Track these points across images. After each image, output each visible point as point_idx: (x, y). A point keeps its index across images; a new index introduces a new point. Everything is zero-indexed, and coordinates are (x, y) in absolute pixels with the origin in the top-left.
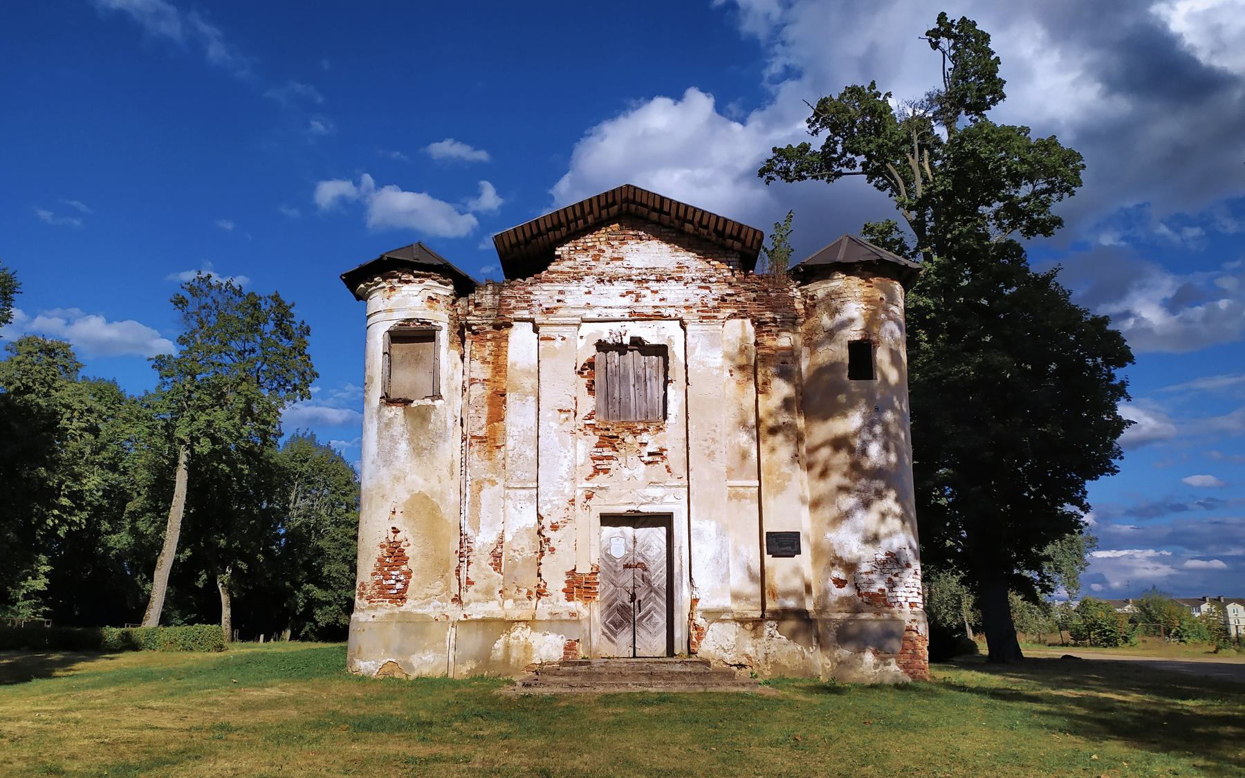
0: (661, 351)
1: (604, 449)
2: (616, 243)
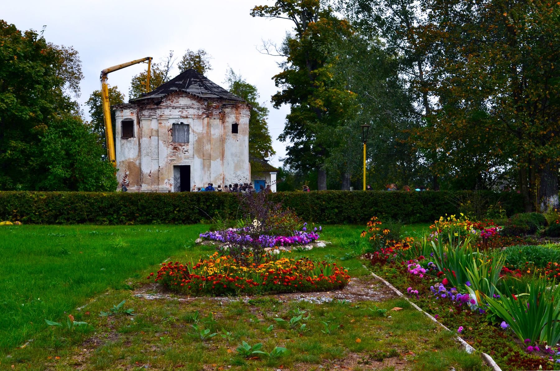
0: (188, 125)
2: (177, 98)
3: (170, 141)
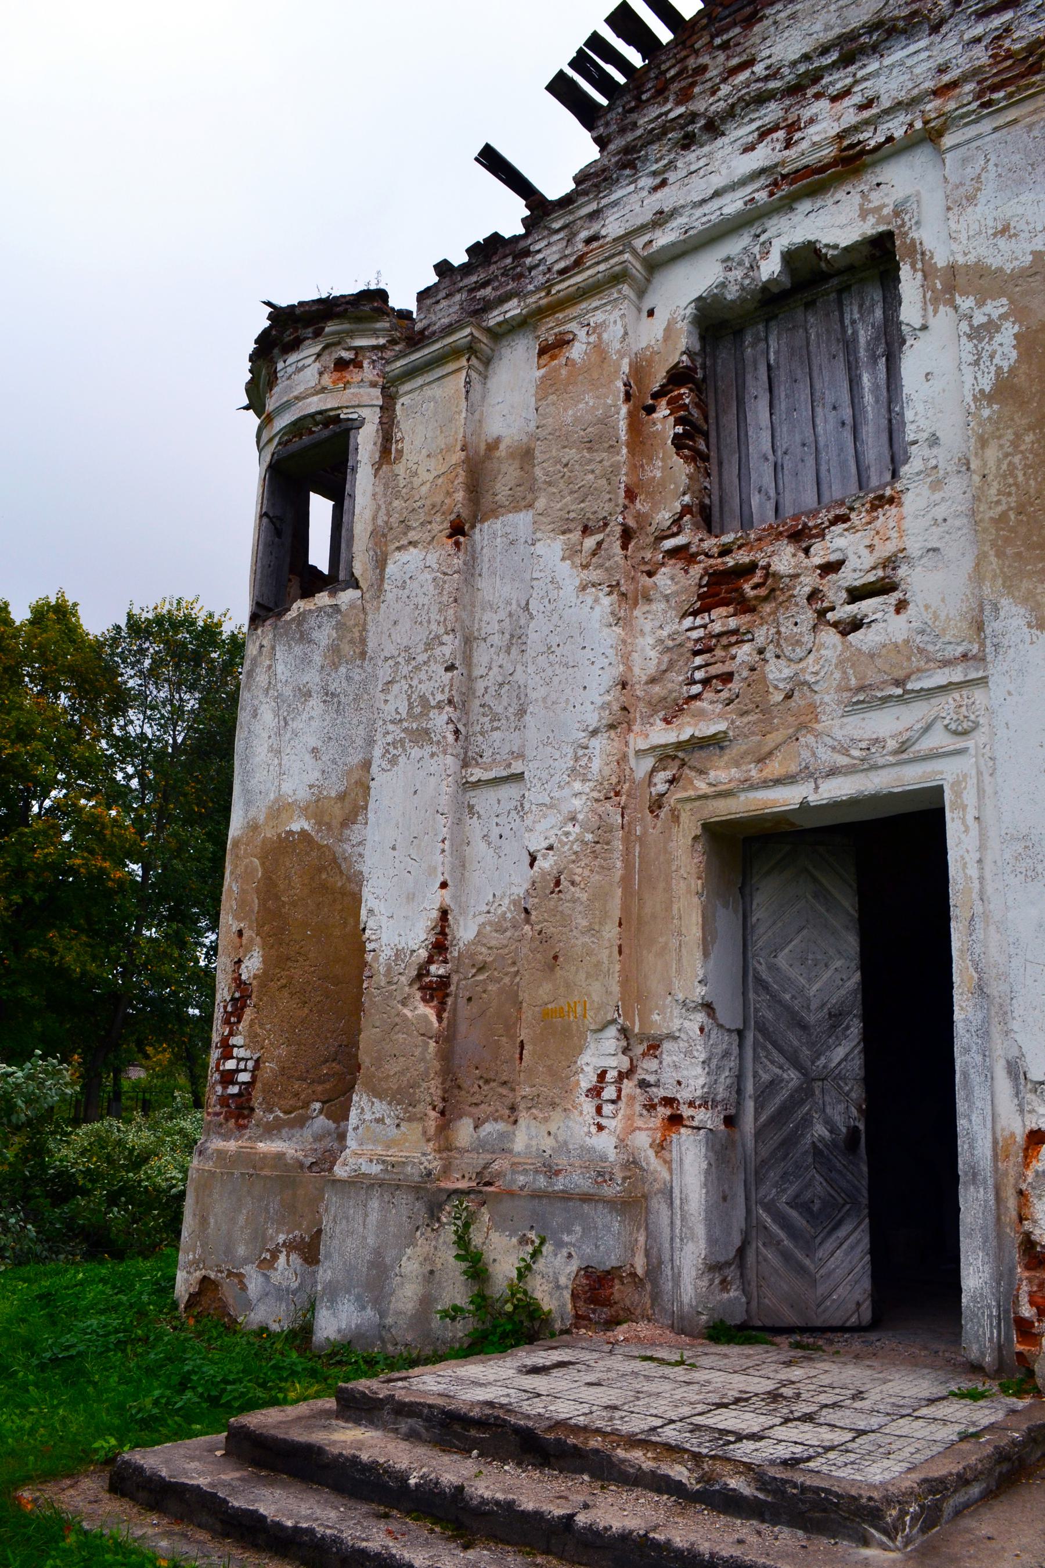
1: (715, 613)
3: (664, 517)
